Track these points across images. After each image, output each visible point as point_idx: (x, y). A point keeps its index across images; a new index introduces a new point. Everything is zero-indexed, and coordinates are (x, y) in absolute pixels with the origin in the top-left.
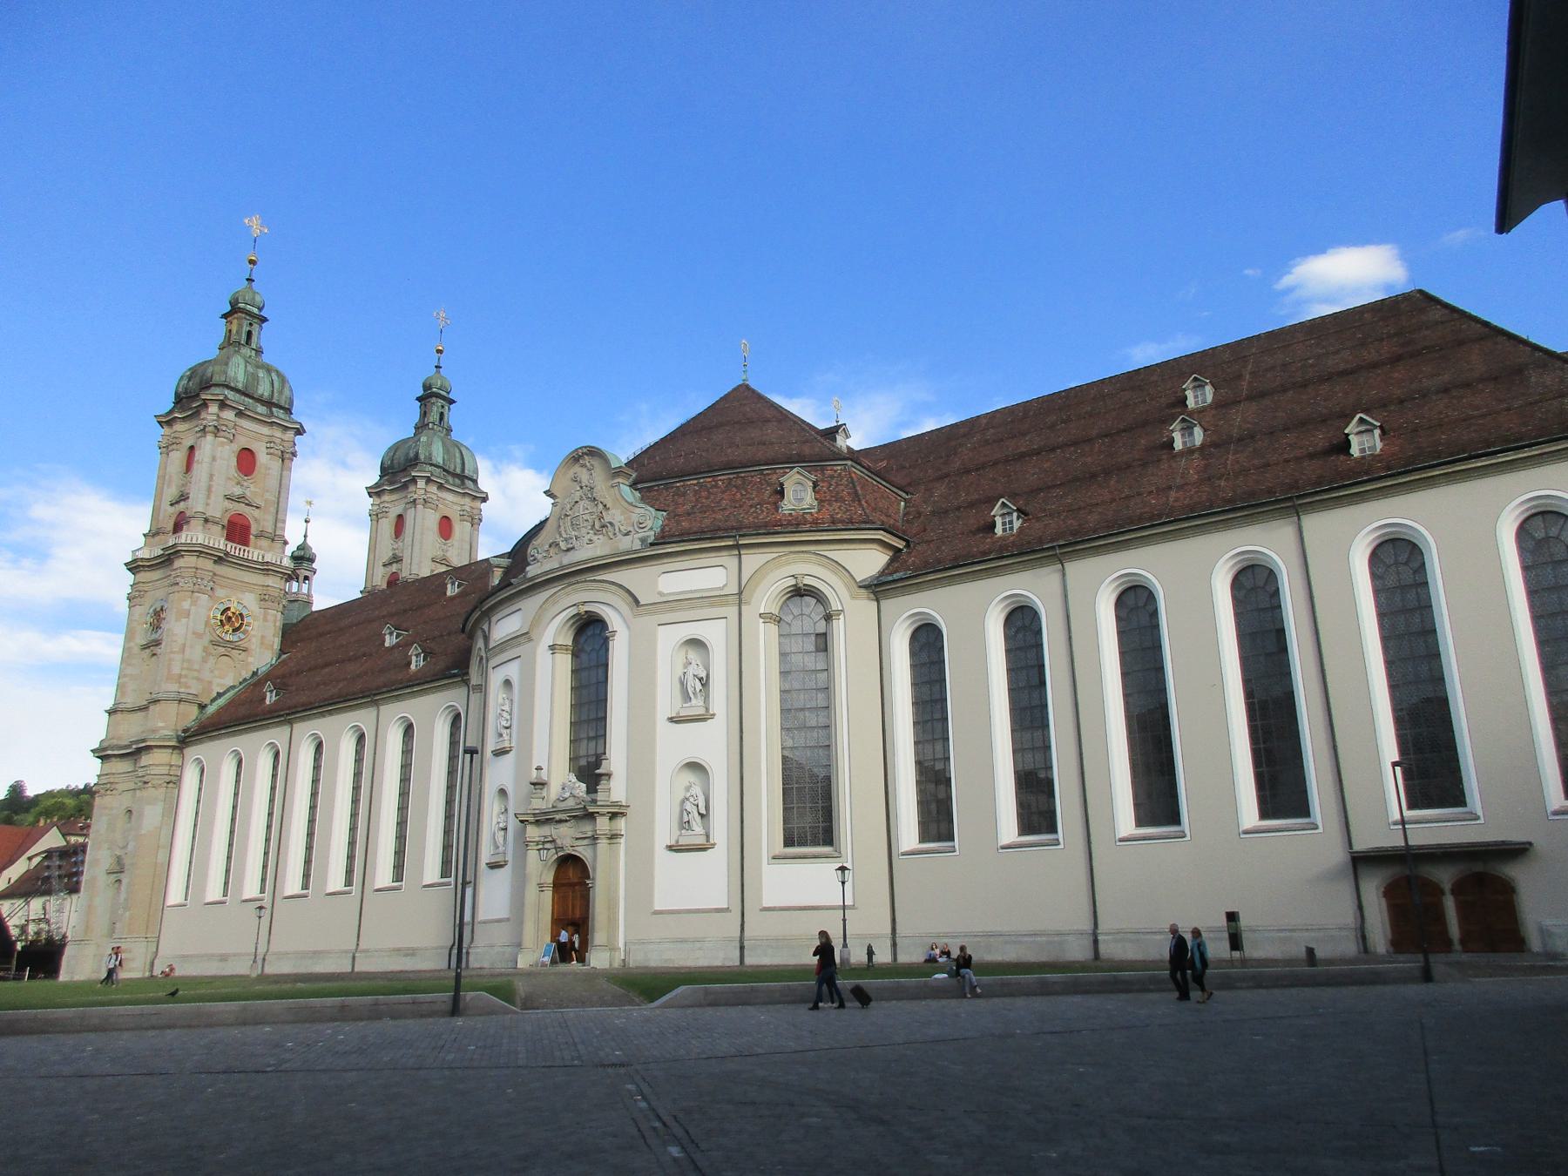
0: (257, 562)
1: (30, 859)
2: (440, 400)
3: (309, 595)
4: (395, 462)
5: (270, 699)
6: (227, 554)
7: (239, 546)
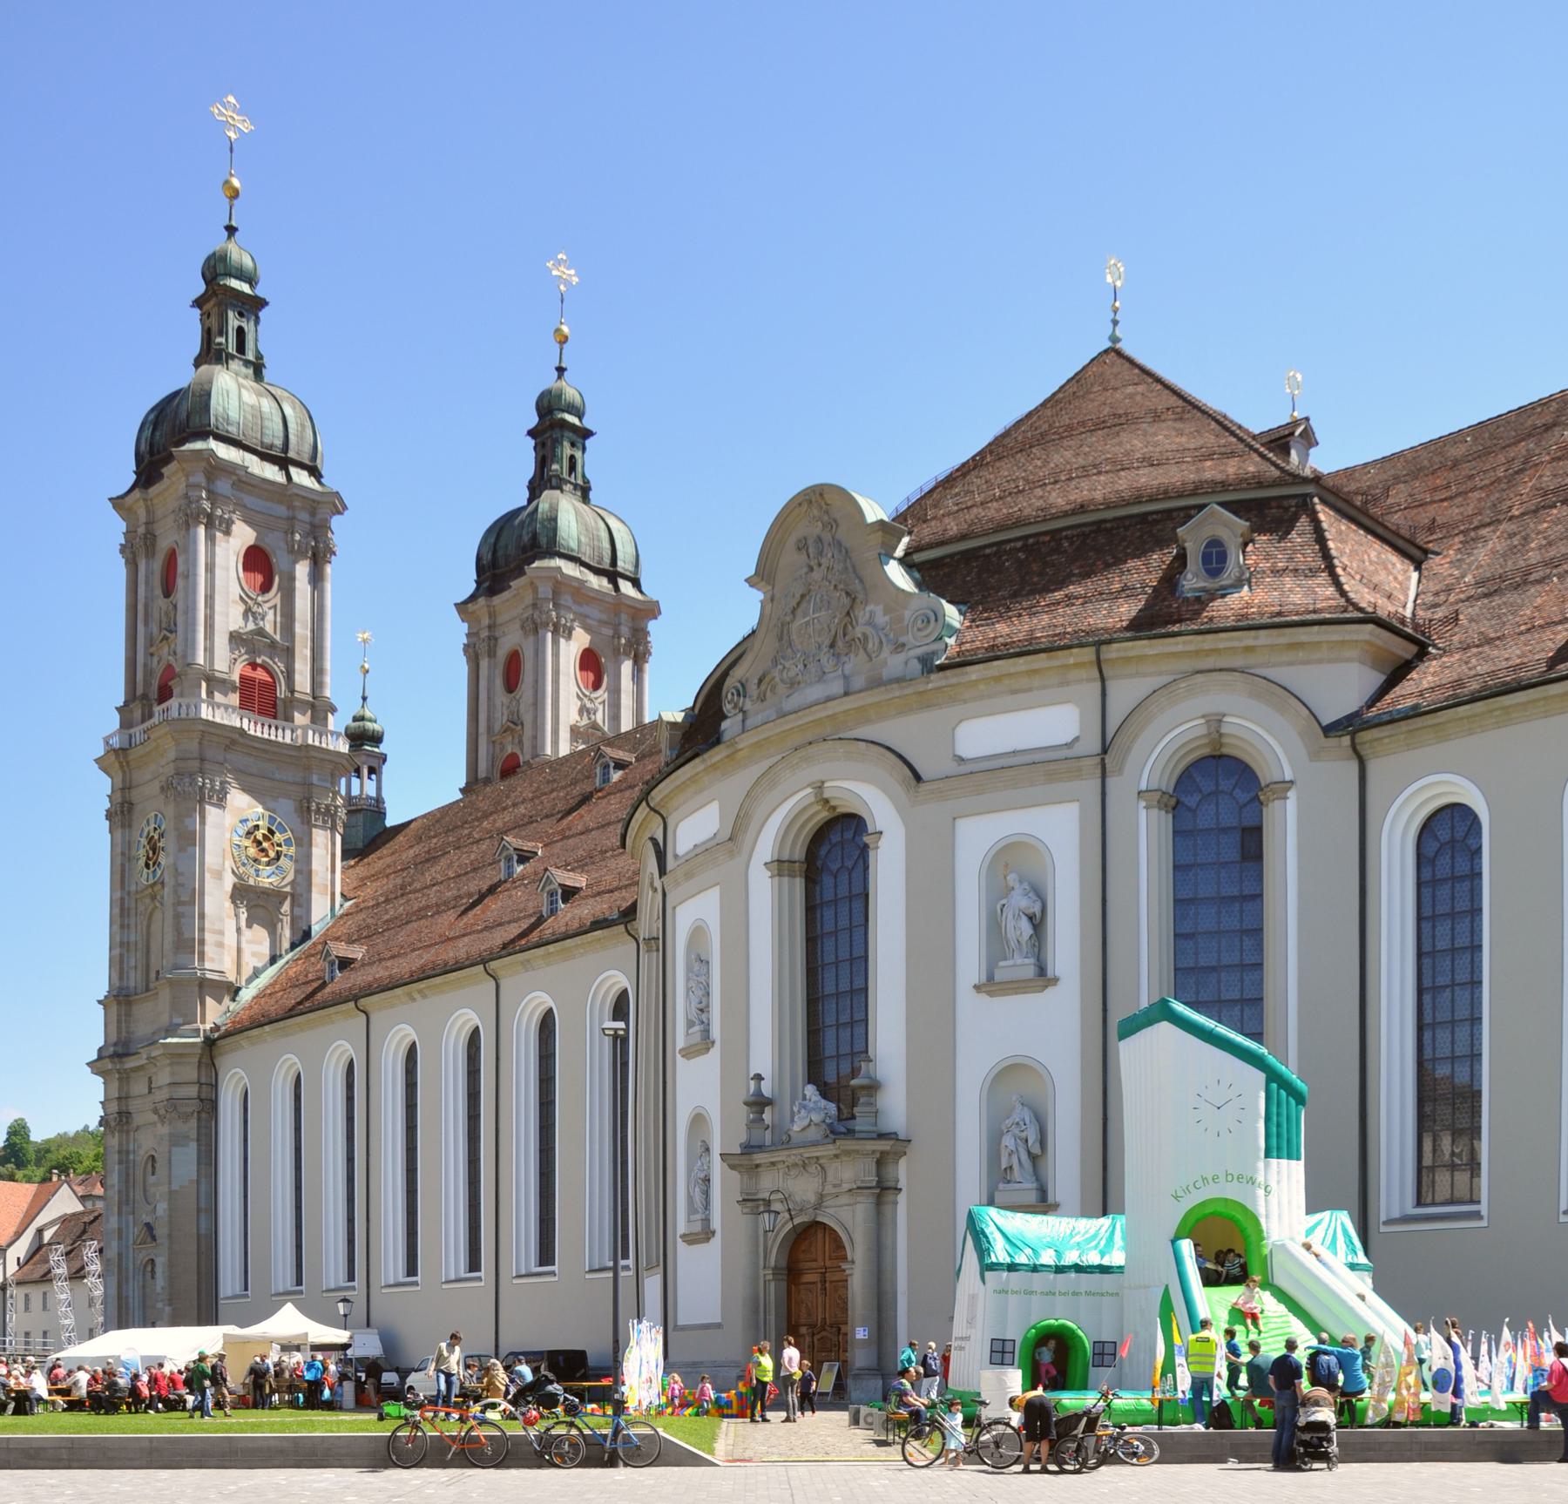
3: (379, 800)
4: (500, 553)
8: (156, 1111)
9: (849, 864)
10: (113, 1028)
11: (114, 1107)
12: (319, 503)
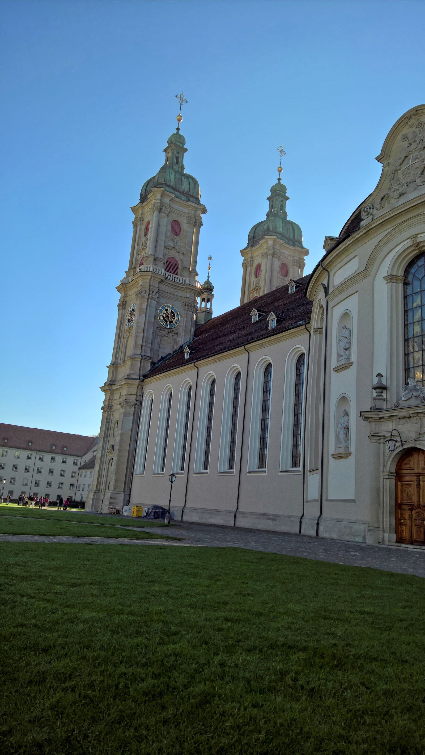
1: (94, 452)
3: (211, 309)
4: (256, 234)
5: (187, 356)
7: (172, 275)
8: (120, 404)
10: (111, 376)
11: (107, 403)
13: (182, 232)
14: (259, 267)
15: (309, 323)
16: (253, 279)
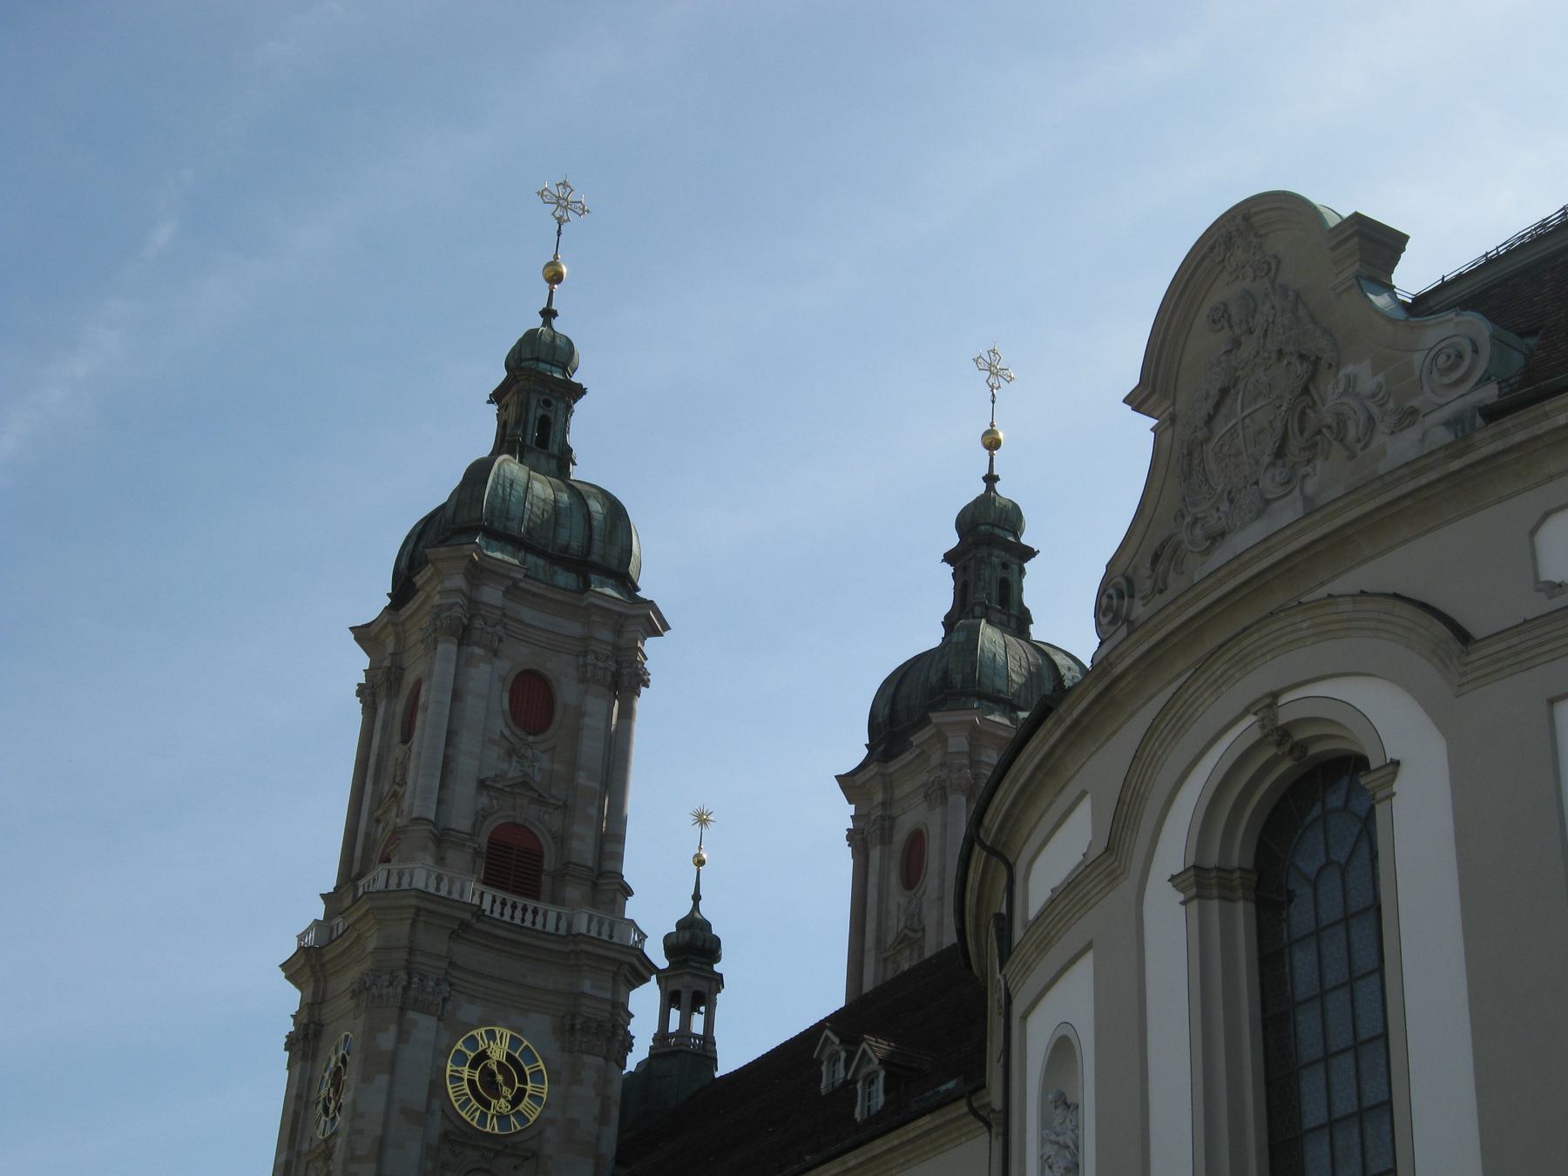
0: (554, 936)
2: (996, 552)
3: (708, 1038)
6: (478, 912)
7: (511, 898)
9: (1340, 855)
12: (627, 617)
13: (558, 717)
14: (917, 841)
15: (983, 1086)
16: (897, 898)
